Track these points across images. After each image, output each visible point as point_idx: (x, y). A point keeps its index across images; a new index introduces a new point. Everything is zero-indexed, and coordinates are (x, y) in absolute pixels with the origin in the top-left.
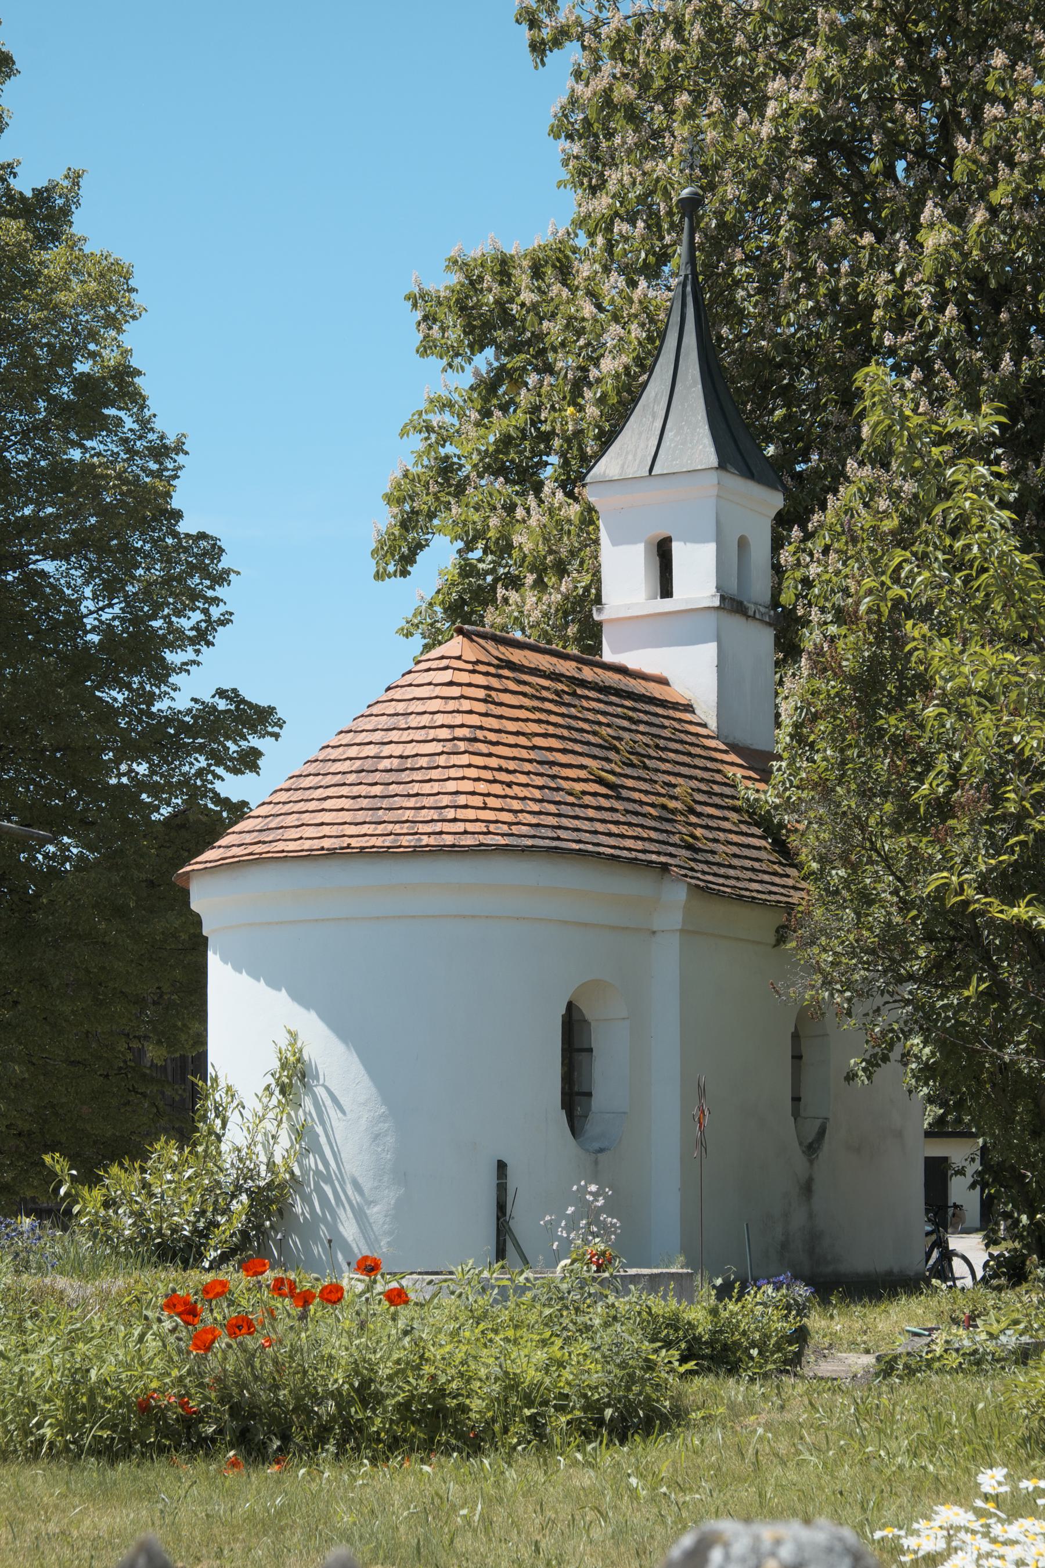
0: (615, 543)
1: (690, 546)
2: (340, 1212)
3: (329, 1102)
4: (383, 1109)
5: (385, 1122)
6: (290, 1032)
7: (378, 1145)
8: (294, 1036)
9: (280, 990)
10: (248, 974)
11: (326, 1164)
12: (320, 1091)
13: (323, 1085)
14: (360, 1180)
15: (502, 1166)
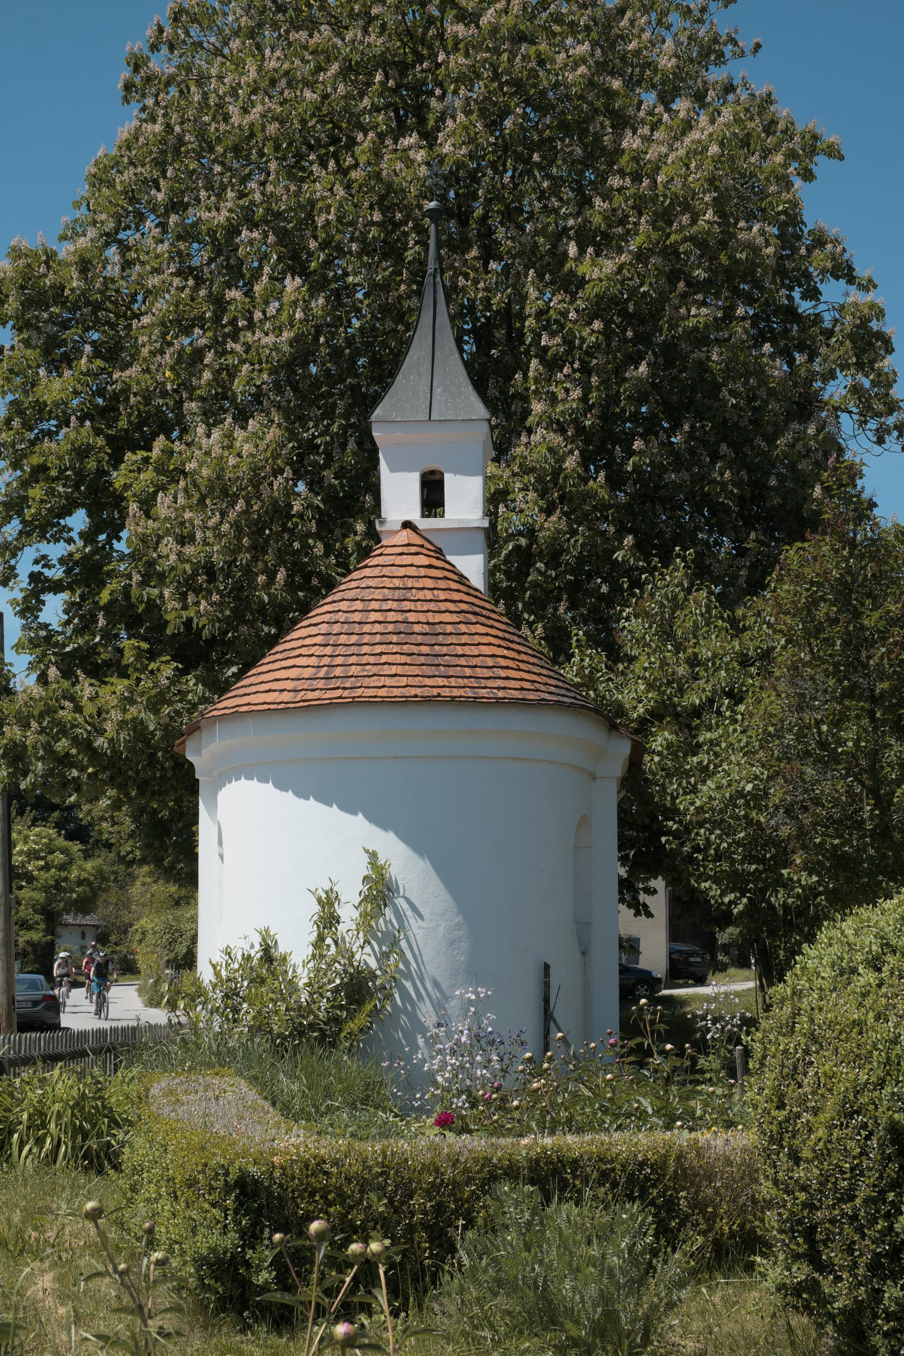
0: (393, 469)
1: (459, 477)
2: (421, 1006)
3: (409, 913)
4: (459, 919)
5: (459, 929)
6: (367, 851)
7: (454, 950)
8: (373, 855)
9: (356, 814)
10: (316, 799)
11: (407, 963)
12: (400, 902)
13: (404, 897)
14: (439, 979)
15: (547, 967)
